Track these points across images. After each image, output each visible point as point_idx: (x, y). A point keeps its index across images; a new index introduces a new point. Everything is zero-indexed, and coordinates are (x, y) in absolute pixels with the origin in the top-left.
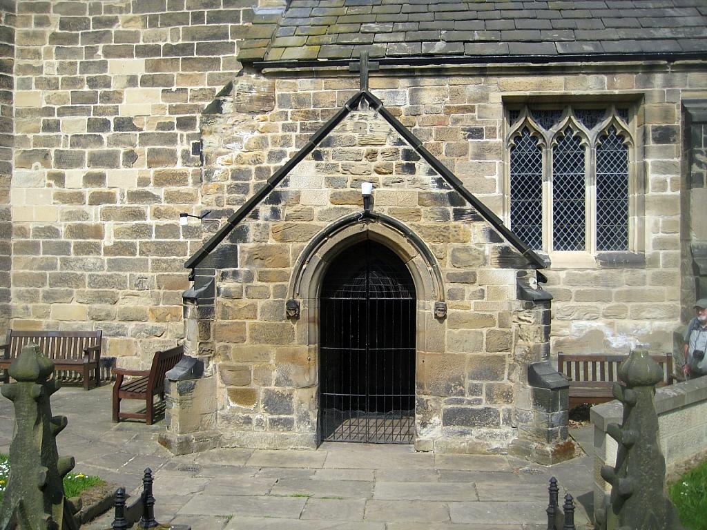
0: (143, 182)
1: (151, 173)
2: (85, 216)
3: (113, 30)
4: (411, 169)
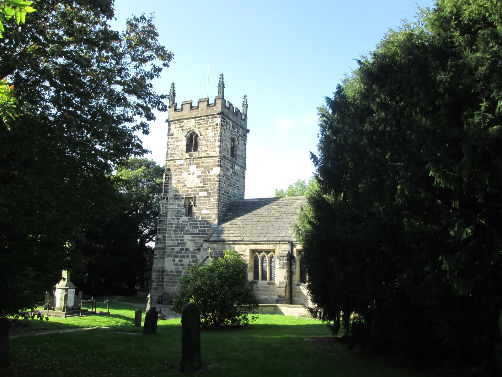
0: (190, 262)
1: (192, 260)
2: (178, 268)
3: (185, 229)
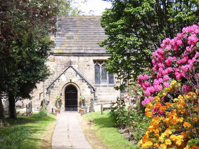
4: (77, 76)
